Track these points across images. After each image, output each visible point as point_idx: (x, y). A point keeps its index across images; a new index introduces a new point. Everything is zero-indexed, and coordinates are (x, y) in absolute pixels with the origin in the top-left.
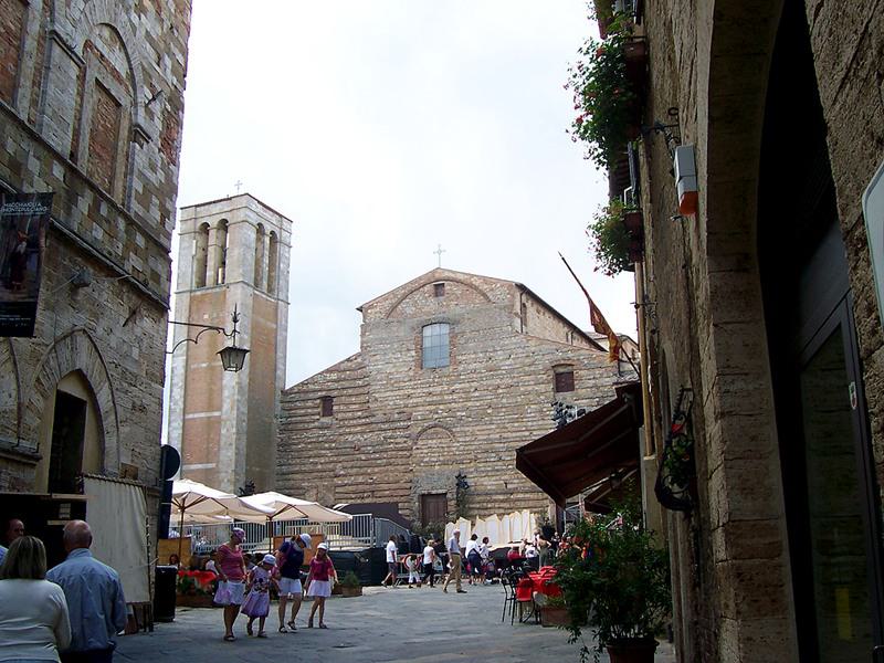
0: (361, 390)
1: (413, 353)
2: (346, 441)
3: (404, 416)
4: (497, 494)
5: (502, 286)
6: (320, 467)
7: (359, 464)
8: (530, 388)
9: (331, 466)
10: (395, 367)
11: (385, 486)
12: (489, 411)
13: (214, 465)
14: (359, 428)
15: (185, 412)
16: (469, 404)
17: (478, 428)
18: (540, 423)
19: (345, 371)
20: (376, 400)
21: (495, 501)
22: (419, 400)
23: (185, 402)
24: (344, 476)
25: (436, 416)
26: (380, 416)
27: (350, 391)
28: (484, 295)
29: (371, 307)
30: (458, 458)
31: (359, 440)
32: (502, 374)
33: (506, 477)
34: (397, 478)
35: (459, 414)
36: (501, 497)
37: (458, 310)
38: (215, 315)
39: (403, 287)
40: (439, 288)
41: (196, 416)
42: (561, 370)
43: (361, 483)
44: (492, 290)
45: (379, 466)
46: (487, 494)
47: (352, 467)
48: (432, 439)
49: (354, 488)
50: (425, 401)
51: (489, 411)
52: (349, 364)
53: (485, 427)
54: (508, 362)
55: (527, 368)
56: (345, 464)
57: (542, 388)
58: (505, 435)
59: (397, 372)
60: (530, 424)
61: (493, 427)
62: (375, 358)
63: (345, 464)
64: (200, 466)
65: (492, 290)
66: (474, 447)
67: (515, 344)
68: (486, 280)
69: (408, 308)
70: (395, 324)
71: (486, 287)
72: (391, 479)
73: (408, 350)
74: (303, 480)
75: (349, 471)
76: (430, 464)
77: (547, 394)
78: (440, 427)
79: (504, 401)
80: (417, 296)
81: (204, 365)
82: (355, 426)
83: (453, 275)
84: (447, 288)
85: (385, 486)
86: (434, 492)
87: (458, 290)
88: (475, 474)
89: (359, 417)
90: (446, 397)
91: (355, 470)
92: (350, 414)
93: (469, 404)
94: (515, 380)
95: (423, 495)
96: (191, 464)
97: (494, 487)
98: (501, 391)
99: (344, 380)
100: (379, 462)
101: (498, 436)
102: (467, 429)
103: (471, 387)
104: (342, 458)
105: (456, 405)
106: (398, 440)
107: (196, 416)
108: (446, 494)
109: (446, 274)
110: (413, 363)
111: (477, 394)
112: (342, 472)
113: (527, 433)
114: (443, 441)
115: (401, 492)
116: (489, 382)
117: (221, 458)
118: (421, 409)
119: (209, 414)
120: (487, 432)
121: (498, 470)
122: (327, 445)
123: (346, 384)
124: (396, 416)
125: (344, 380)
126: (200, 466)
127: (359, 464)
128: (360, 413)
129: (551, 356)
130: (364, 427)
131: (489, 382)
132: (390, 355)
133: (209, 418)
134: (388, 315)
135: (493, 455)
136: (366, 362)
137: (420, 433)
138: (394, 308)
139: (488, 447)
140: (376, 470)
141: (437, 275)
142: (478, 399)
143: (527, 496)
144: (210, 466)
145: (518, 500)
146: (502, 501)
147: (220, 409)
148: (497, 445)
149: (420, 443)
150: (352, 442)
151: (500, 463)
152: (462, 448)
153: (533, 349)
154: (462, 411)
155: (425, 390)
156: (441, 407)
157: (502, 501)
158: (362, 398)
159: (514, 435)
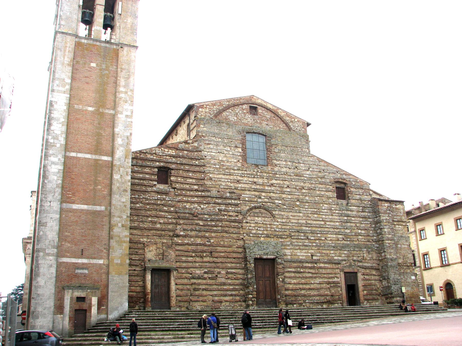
0: (197, 169)
1: (240, 150)
2: (185, 208)
3: (234, 196)
4: (307, 262)
5: (298, 121)
6: (158, 226)
7: (197, 228)
8: (323, 193)
9: (170, 227)
10: (226, 156)
11: (219, 249)
12: (298, 203)
13: (103, 208)
14: (196, 199)
15: (67, 148)
16: (284, 196)
17: (291, 214)
18: (330, 217)
19: (183, 150)
20: (211, 179)
21: (306, 267)
22: (246, 186)
23: (67, 138)
24: (185, 236)
25: (259, 200)
26: (214, 193)
27: (187, 167)
28: (287, 125)
29: (202, 107)
30: (277, 233)
31: (197, 209)
32: (305, 180)
33: (313, 251)
34: (231, 244)
35: (276, 201)
36: (310, 265)
37: (268, 128)
38: (104, 66)
39: (229, 100)
40: (253, 109)
41: (80, 155)
42: (338, 186)
43: (200, 245)
44: (292, 122)
45: (215, 232)
46: (300, 262)
47: (192, 230)
48: (258, 217)
49: (194, 248)
50: (251, 188)
51: (298, 203)
52: (187, 146)
53: (296, 214)
54: (308, 173)
55: (320, 179)
56: (185, 227)
57: (330, 194)
58: (309, 222)
59: (228, 162)
60: (324, 216)
61: (301, 215)
62: (209, 146)
63: (185, 227)
64: (85, 207)
65: (292, 122)
66: (288, 227)
67: (312, 161)
68: (288, 115)
69: (230, 115)
70: (224, 124)
71: (288, 118)
72: (226, 243)
73: (236, 147)
74: (143, 236)
75: (189, 233)
76: (257, 236)
77: (334, 199)
78: (265, 209)
79: (307, 198)
80: (237, 110)
81: (90, 109)
82: (192, 196)
83: (265, 104)
84: (260, 111)
85: (219, 249)
86: (265, 257)
87: (268, 115)
88: (291, 247)
89: (196, 190)
90: (266, 188)
91: (193, 233)
92: (188, 186)
93: (284, 196)
94: (313, 186)
95: (256, 259)
96: (73, 203)
97: (304, 258)
98: (304, 191)
99: (183, 157)
100: (215, 228)
101: (304, 222)
102: (283, 213)
103: (284, 184)
104: (182, 222)
105: (274, 195)
106: (231, 214)
107: (80, 155)
108: (274, 260)
109: (259, 101)
110: (240, 157)
111: (288, 190)
112: (182, 233)
113: (323, 223)
114: (266, 219)
115: (235, 255)
116: (296, 183)
117: (114, 202)
118: (248, 192)
119: (97, 157)
120: (297, 218)
121: (306, 246)
122: (165, 208)
123: (184, 161)
124: (228, 195)
125: (183, 157)
126: (85, 207)
127: (197, 228)
128: (196, 187)
129: (333, 175)
130: (200, 199)
131: (296, 183)
132: (221, 147)
133: (96, 160)
134: (216, 116)
135: (302, 235)
136: (202, 148)
137: (248, 210)
138: (220, 112)
139: (299, 228)
140: (213, 235)
141: (253, 100)
142: (290, 193)
143: (327, 265)
144: (98, 208)
145: (321, 268)
146: (310, 268)
147: (112, 154)
148: (304, 228)
149: (249, 218)
150: (190, 209)
151: (307, 241)
152: (280, 227)
153: (323, 168)
154: (279, 200)
155: (250, 180)
156: (263, 194)
157: (310, 268)
158: (198, 175)
159: (315, 222)
